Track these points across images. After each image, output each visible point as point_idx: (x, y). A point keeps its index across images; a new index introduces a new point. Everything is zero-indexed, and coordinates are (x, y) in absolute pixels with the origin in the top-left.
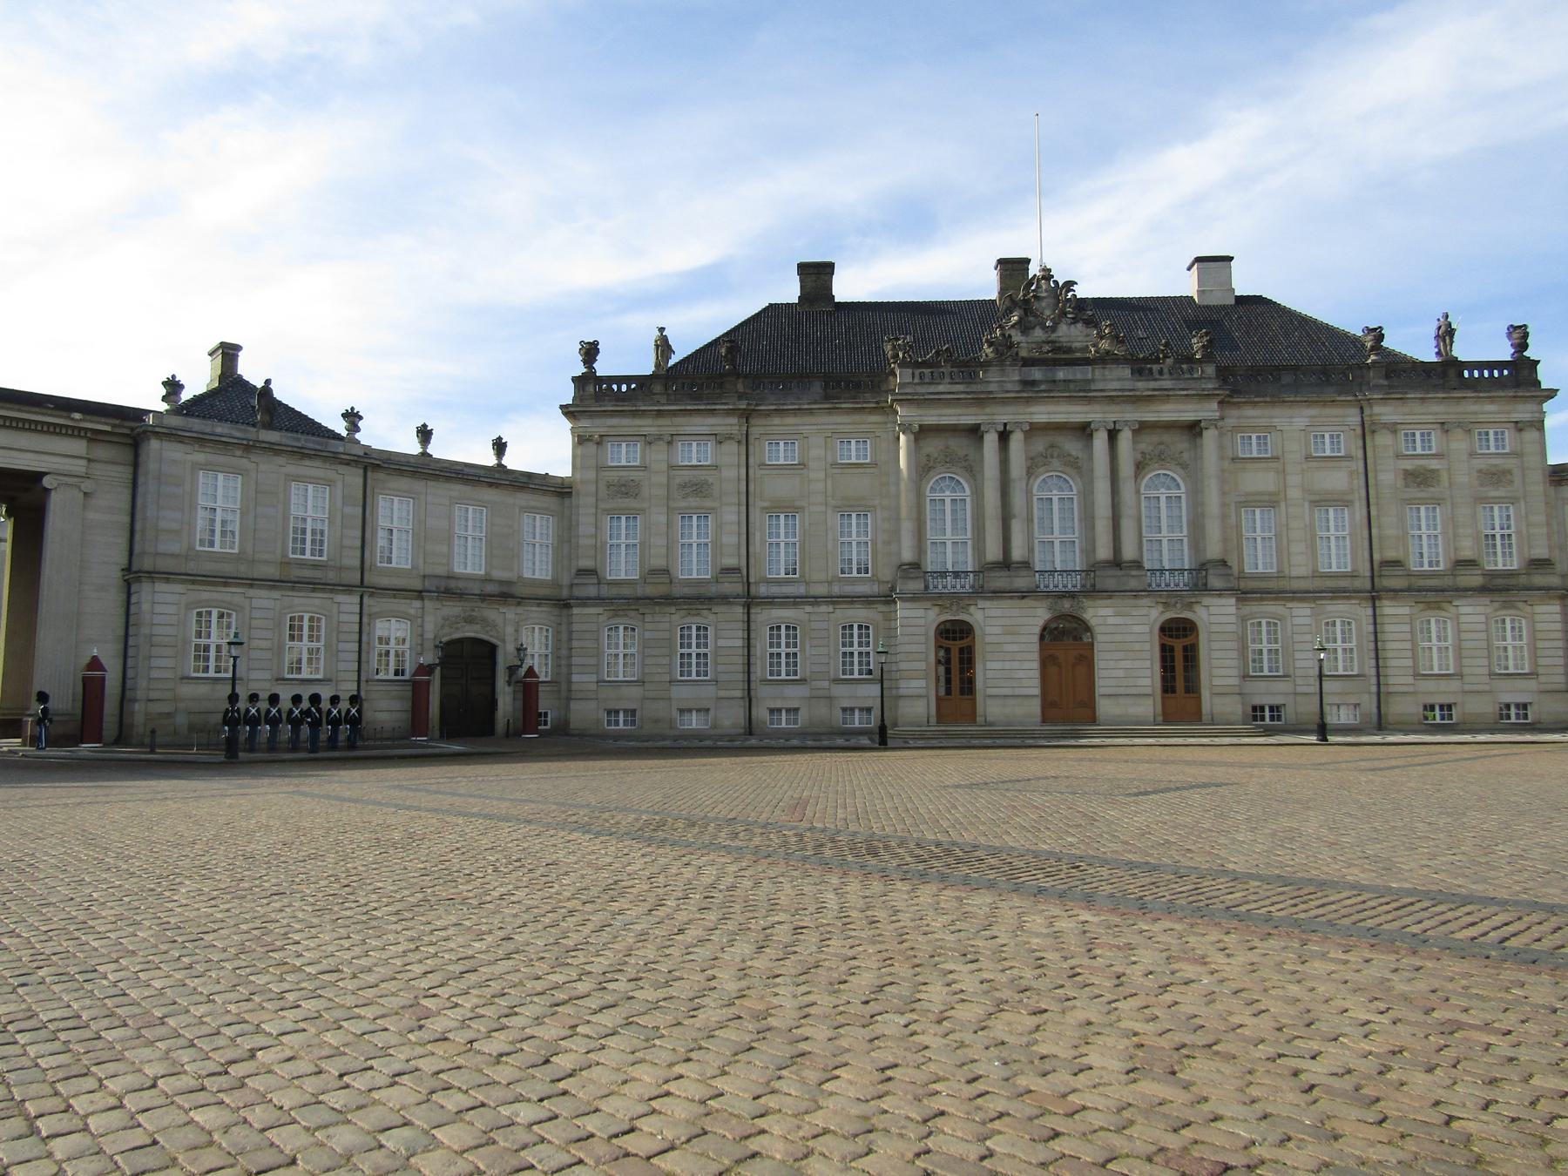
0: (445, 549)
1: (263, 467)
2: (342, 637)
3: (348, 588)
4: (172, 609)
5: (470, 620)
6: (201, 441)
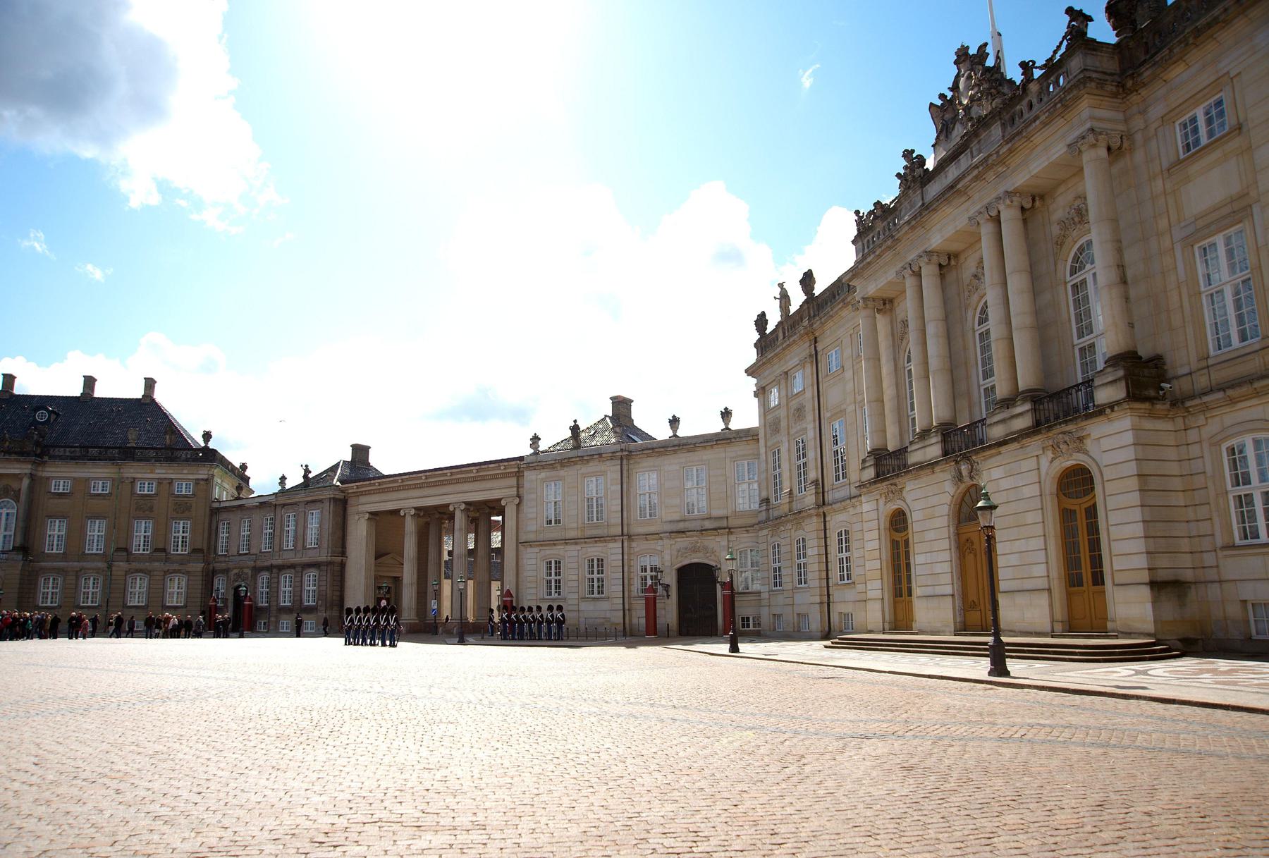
3: (613, 538)
5: (695, 550)
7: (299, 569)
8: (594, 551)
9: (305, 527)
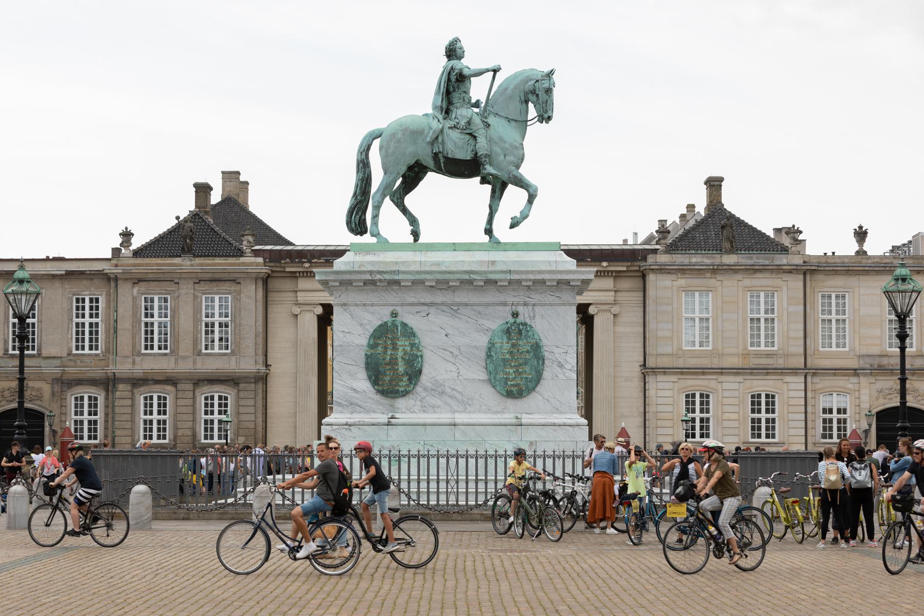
0: (877, 332)
1: (726, 283)
2: (791, 409)
3: (794, 371)
4: (669, 393)
6: (682, 271)
7: (190, 387)
8: (762, 385)
9: (197, 320)
